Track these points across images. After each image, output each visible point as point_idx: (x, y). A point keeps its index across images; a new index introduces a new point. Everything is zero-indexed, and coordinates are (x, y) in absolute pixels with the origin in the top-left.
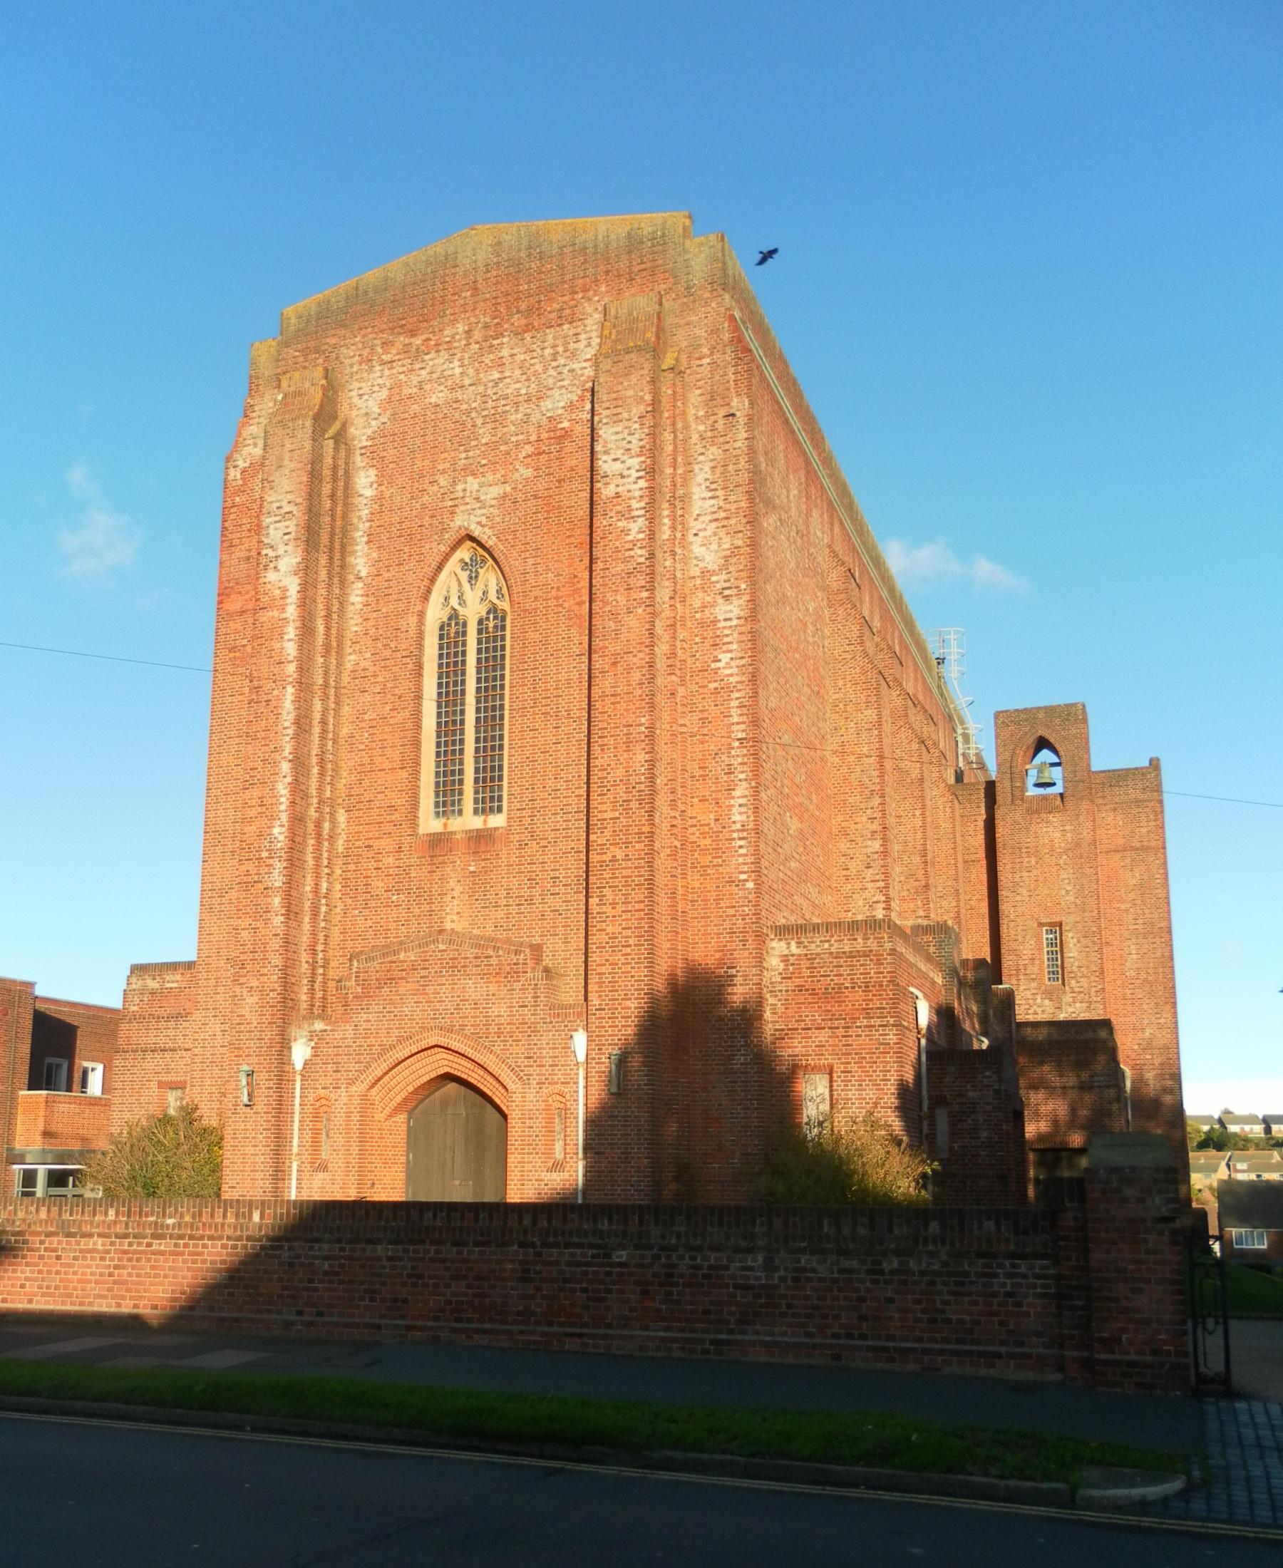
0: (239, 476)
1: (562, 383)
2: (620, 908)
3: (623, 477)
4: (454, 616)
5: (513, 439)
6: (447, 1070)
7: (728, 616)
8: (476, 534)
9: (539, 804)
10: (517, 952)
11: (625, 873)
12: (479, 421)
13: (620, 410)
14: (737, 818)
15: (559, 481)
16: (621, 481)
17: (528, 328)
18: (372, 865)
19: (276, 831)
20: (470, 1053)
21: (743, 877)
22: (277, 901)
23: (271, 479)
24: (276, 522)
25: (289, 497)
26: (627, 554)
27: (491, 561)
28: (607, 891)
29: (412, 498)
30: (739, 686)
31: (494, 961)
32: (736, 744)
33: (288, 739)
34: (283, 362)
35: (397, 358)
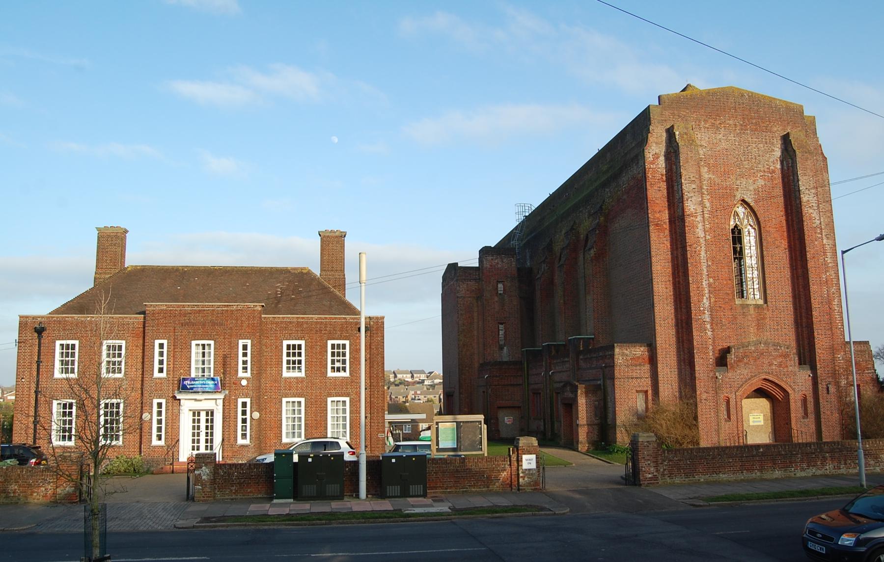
0: (651, 157)
1: (770, 153)
2: (824, 336)
3: (809, 195)
4: (736, 226)
5: (755, 168)
6: (761, 386)
7: (829, 244)
8: (746, 200)
9: (777, 298)
10: (787, 348)
11: (824, 325)
12: (743, 159)
13: (805, 172)
14: (836, 308)
15: (773, 187)
16: (809, 196)
17: (756, 130)
18: (722, 313)
19: (705, 301)
20: (776, 381)
21: (840, 327)
22: (708, 326)
23: (685, 166)
24: (689, 183)
25: (694, 175)
26: (814, 221)
27: (749, 210)
28: (819, 331)
29: (722, 181)
30: (834, 267)
31: (780, 351)
32: (835, 285)
33: (705, 267)
34: (664, 116)
35: (710, 127)
